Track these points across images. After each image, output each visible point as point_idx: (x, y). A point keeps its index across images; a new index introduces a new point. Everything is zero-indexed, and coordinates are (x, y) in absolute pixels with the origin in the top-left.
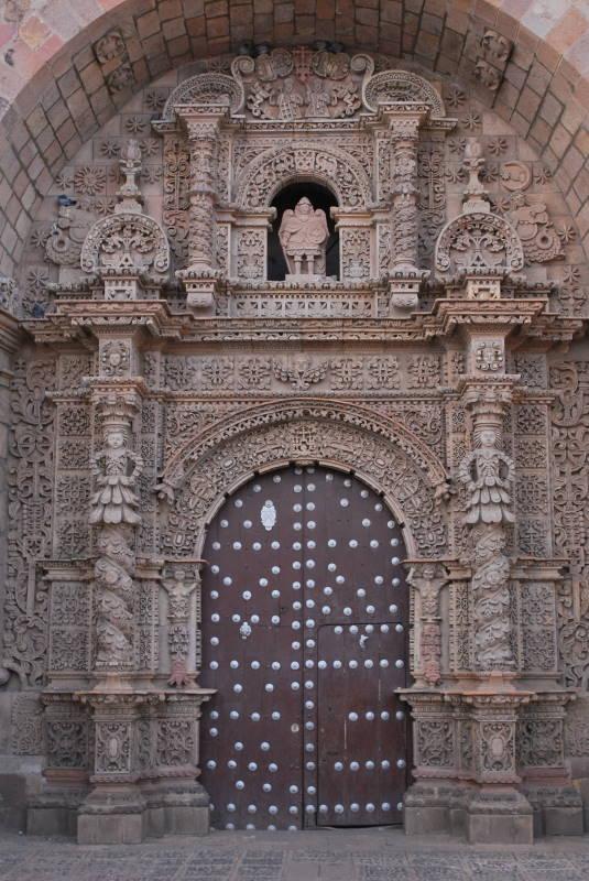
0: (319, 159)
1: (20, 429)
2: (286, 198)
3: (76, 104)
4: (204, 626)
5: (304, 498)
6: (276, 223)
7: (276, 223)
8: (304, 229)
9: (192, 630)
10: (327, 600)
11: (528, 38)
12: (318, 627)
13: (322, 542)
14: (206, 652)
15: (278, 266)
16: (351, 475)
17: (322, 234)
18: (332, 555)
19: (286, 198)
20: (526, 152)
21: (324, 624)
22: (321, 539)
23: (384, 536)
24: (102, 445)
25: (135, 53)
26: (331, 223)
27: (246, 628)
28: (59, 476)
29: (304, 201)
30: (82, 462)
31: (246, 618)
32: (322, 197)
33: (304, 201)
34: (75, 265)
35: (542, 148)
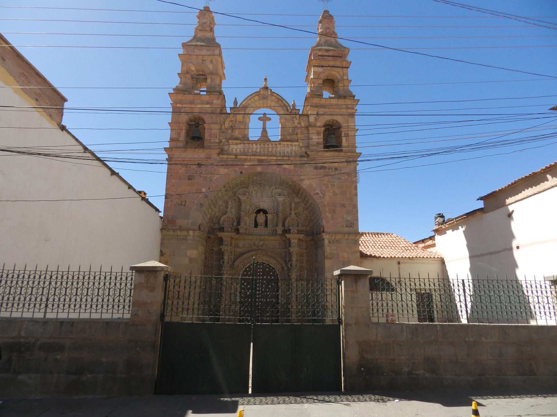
0: (264, 205)
2: (259, 211)
3: (220, 194)
4: (241, 292)
5: (260, 268)
6: (256, 216)
7: (256, 216)
8: (261, 218)
12: (262, 293)
13: (263, 277)
14: (241, 297)
15: (256, 225)
16: (269, 265)
18: (264, 280)
19: (259, 211)
20: (303, 205)
21: (263, 292)
22: (263, 276)
23: (273, 275)
24: (223, 258)
25: (231, 185)
26: (266, 217)
27: (248, 293)
29: (261, 213)
31: (248, 291)
32: (265, 212)
33: (261, 213)
34: (219, 223)
35: (306, 205)
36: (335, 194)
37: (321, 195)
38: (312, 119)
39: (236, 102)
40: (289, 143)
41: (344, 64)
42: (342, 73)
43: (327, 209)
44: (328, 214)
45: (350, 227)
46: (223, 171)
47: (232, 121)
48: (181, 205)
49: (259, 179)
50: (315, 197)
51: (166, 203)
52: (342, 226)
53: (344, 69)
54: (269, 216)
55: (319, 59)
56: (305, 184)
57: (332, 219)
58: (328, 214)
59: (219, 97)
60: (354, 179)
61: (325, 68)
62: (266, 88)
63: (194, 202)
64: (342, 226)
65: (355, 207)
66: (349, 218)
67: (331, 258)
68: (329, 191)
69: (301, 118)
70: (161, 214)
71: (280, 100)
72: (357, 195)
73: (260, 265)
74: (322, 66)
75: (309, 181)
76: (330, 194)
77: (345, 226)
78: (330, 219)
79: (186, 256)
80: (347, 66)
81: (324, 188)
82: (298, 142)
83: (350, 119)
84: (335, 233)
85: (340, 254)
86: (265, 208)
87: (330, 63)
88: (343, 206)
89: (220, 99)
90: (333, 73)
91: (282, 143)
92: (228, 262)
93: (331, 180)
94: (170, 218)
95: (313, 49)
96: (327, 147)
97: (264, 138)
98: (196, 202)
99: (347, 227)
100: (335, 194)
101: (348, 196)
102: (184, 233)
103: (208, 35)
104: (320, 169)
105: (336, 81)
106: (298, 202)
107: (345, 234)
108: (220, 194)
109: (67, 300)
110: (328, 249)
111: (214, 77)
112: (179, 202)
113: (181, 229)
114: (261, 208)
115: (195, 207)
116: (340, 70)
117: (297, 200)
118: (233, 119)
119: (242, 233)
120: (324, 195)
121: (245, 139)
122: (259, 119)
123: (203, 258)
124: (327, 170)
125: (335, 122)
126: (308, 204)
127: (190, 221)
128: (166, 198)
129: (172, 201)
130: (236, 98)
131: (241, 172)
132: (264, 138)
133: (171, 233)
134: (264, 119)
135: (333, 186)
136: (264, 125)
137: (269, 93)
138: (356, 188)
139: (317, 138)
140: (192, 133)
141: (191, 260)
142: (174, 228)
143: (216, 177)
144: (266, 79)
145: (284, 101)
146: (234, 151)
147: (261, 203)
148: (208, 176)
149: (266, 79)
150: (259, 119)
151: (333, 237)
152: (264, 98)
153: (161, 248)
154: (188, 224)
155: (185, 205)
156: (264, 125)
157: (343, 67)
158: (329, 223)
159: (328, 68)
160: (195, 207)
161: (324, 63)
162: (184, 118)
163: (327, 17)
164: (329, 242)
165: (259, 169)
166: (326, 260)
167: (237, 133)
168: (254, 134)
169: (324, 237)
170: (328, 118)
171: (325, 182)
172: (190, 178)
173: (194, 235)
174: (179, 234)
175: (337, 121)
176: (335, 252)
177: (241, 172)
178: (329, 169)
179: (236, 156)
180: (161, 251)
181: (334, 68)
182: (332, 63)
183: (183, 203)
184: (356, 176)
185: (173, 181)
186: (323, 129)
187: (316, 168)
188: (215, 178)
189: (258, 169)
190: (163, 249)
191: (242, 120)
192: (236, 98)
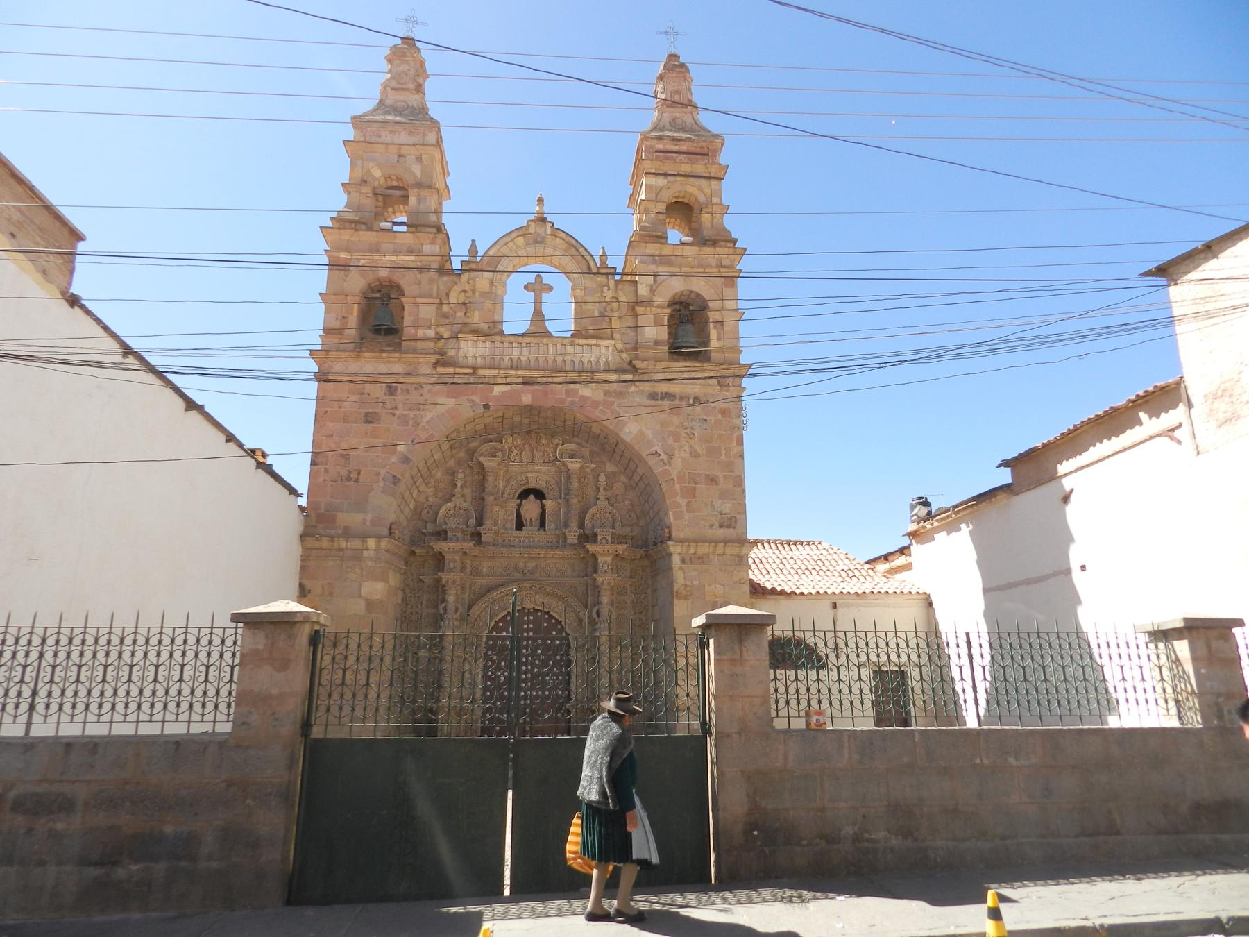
0: (539, 477)
1: (407, 591)
2: (525, 494)
3: (438, 456)
5: (528, 622)
6: (519, 505)
7: (519, 505)
8: (531, 509)
9: (479, 680)
10: (537, 666)
11: (624, 442)
12: (533, 678)
15: (520, 525)
16: (548, 613)
17: (539, 511)
19: (525, 494)
20: (623, 478)
21: (535, 676)
23: (561, 639)
24: (444, 601)
26: (543, 506)
28: (425, 612)
29: (532, 497)
30: (436, 607)
32: (540, 495)
33: (532, 497)
34: (435, 522)
36: (695, 454)
37: (663, 456)
38: (643, 291)
39: (473, 250)
40: (593, 342)
41: (713, 171)
42: (707, 191)
43: (677, 487)
44: (679, 499)
45: (729, 526)
46: (445, 403)
47: (465, 291)
48: (349, 479)
49: (526, 421)
50: (652, 461)
51: (313, 476)
52: (712, 526)
53: (714, 182)
54: (549, 504)
55: (657, 158)
56: (630, 431)
57: (688, 511)
58: (679, 499)
59: (434, 238)
60: (736, 421)
61: (670, 178)
62: (542, 220)
63: (378, 474)
64: (712, 526)
65: (739, 482)
66: (727, 507)
67: (686, 597)
68: (681, 447)
69: (620, 286)
70: (303, 501)
71: (574, 247)
72: (742, 456)
73: (528, 614)
74: (666, 175)
75: (638, 426)
76: (683, 455)
77: (717, 525)
78: (684, 509)
79: (360, 596)
80: (719, 175)
81: (670, 441)
82: (612, 338)
83: (727, 292)
84: (696, 542)
85: (707, 588)
86: (538, 487)
87: (682, 171)
88: (713, 480)
89: (439, 241)
90: (690, 189)
91: (577, 341)
92: (457, 610)
93: (686, 424)
94: (322, 511)
95: (645, 137)
96: (678, 351)
97: (538, 329)
98: (383, 472)
99: (721, 527)
100: (695, 454)
101: (723, 458)
102: (356, 544)
103: (413, 99)
104: (662, 399)
105: (696, 207)
106: (614, 473)
107: (717, 542)
108: (438, 456)
109: (101, 655)
110: (680, 577)
111: (424, 193)
112: (344, 472)
113: (347, 534)
114: (531, 486)
115: (382, 484)
116: (703, 182)
117: (610, 468)
118: (467, 287)
119: (487, 543)
120: (670, 455)
121: (494, 331)
122: (526, 287)
123: (399, 601)
124: (677, 402)
125: (693, 296)
126: (637, 478)
127: (369, 517)
128: (313, 463)
129: (326, 471)
130: (473, 241)
131: (486, 407)
132: (538, 329)
133: (325, 543)
134: (538, 288)
135: (691, 436)
136: (538, 303)
137: (549, 231)
138: (740, 442)
139: (654, 333)
140: (375, 317)
141: (370, 604)
142: (333, 532)
143: (429, 416)
144: (541, 201)
145: (581, 250)
146: (471, 361)
147: (530, 475)
148: (412, 414)
149: (541, 201)
150: (526, 287)
151: (692, 550)
152: (536, 242)
153: (301, 578)
154: (365, 523)
155: (357, 481)
156: (538, 303)
157: (710, 178)
158: (684, 519)
159: (679, 178)
160: (382, 484)
161: (669, 168)
162: (356, 283)
163: (675, 67)
164: (683, 561)
165: (526, 399)
166: (676, 602)
167: (475, 317)
168: (515, 318)
169: (672, 549)
170: (676, 286)
171: (672, 429)
172: (369, 418)
173: (377, 549)
174: (343, 545)
175: (698, 295)
176: (696, 583)
177: (486, 407)
178: (681, 398)
179: (474, 368)
180: (301, 586)
181: (691, 180)
182: (686, 169)
183: (354, 476)
184: (739, 416)
185: (330, 425)
186: (668, 311)
187: (653, 396)
188: (425, 420)
189: (524, 399)
190: (305, 582)
191: (488, 290)
192: (473, 241)
